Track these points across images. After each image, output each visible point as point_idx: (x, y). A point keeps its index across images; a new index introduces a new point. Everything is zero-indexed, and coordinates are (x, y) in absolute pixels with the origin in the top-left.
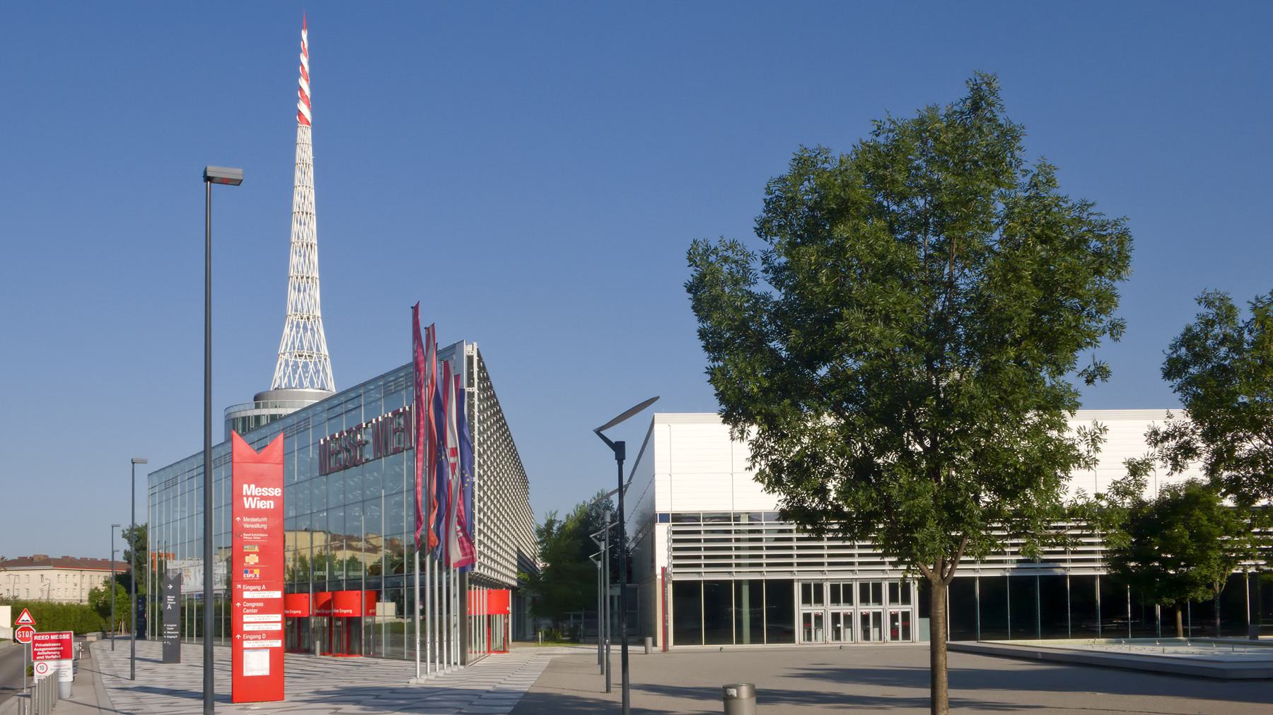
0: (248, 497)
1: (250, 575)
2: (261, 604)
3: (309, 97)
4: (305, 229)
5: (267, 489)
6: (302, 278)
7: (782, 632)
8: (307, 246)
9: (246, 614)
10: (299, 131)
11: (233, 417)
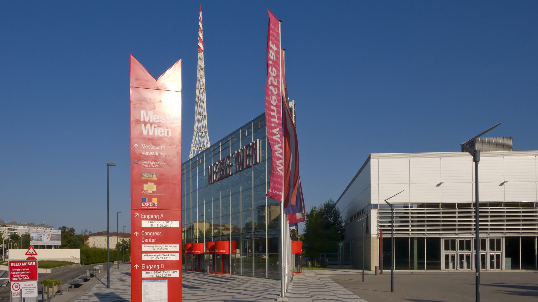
3: (203, 40)
6: (200, 115)
7: (434, 263)
8: (202, 102)
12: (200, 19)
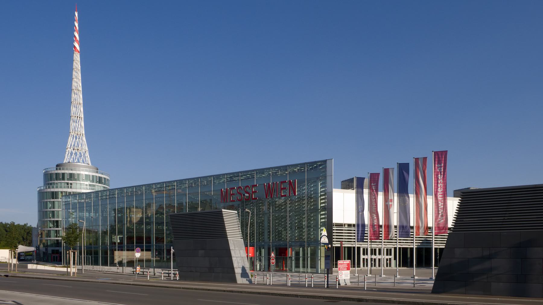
3: (79, 40)
4: (78, 97)
6: (77, 117)
8: (79, 104)
10: (75, 55)
11: (48, 173)
12: (76, 19)
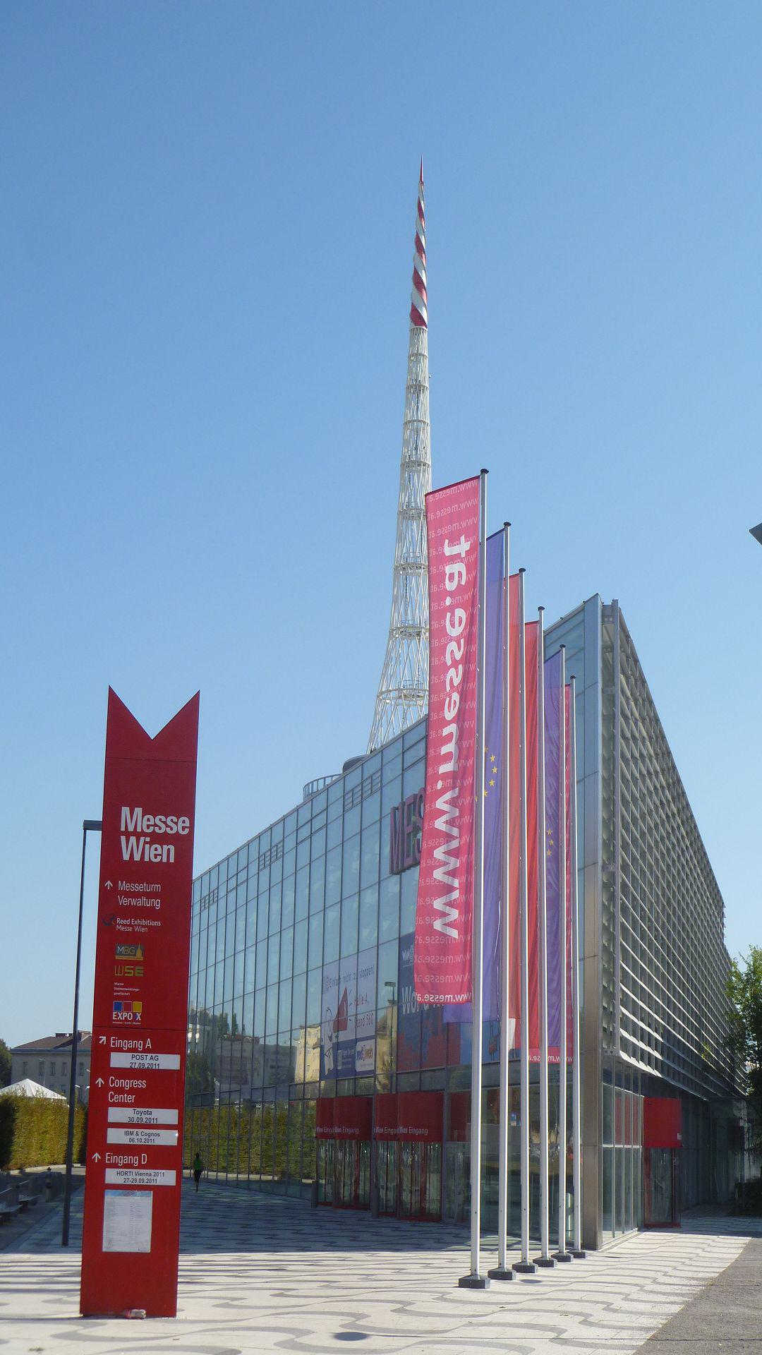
0: (128, 834)
1: (125, 1015)
2: (142, 1084)
5: (163, 818)
9: (115, 1105)
